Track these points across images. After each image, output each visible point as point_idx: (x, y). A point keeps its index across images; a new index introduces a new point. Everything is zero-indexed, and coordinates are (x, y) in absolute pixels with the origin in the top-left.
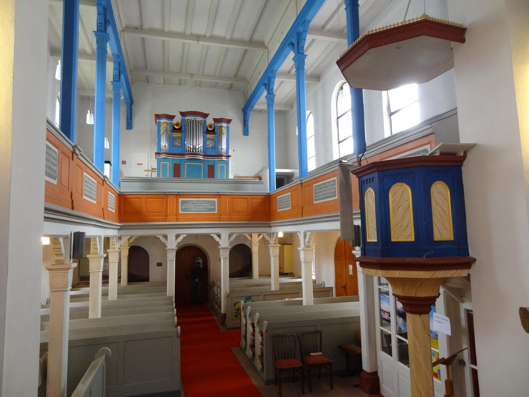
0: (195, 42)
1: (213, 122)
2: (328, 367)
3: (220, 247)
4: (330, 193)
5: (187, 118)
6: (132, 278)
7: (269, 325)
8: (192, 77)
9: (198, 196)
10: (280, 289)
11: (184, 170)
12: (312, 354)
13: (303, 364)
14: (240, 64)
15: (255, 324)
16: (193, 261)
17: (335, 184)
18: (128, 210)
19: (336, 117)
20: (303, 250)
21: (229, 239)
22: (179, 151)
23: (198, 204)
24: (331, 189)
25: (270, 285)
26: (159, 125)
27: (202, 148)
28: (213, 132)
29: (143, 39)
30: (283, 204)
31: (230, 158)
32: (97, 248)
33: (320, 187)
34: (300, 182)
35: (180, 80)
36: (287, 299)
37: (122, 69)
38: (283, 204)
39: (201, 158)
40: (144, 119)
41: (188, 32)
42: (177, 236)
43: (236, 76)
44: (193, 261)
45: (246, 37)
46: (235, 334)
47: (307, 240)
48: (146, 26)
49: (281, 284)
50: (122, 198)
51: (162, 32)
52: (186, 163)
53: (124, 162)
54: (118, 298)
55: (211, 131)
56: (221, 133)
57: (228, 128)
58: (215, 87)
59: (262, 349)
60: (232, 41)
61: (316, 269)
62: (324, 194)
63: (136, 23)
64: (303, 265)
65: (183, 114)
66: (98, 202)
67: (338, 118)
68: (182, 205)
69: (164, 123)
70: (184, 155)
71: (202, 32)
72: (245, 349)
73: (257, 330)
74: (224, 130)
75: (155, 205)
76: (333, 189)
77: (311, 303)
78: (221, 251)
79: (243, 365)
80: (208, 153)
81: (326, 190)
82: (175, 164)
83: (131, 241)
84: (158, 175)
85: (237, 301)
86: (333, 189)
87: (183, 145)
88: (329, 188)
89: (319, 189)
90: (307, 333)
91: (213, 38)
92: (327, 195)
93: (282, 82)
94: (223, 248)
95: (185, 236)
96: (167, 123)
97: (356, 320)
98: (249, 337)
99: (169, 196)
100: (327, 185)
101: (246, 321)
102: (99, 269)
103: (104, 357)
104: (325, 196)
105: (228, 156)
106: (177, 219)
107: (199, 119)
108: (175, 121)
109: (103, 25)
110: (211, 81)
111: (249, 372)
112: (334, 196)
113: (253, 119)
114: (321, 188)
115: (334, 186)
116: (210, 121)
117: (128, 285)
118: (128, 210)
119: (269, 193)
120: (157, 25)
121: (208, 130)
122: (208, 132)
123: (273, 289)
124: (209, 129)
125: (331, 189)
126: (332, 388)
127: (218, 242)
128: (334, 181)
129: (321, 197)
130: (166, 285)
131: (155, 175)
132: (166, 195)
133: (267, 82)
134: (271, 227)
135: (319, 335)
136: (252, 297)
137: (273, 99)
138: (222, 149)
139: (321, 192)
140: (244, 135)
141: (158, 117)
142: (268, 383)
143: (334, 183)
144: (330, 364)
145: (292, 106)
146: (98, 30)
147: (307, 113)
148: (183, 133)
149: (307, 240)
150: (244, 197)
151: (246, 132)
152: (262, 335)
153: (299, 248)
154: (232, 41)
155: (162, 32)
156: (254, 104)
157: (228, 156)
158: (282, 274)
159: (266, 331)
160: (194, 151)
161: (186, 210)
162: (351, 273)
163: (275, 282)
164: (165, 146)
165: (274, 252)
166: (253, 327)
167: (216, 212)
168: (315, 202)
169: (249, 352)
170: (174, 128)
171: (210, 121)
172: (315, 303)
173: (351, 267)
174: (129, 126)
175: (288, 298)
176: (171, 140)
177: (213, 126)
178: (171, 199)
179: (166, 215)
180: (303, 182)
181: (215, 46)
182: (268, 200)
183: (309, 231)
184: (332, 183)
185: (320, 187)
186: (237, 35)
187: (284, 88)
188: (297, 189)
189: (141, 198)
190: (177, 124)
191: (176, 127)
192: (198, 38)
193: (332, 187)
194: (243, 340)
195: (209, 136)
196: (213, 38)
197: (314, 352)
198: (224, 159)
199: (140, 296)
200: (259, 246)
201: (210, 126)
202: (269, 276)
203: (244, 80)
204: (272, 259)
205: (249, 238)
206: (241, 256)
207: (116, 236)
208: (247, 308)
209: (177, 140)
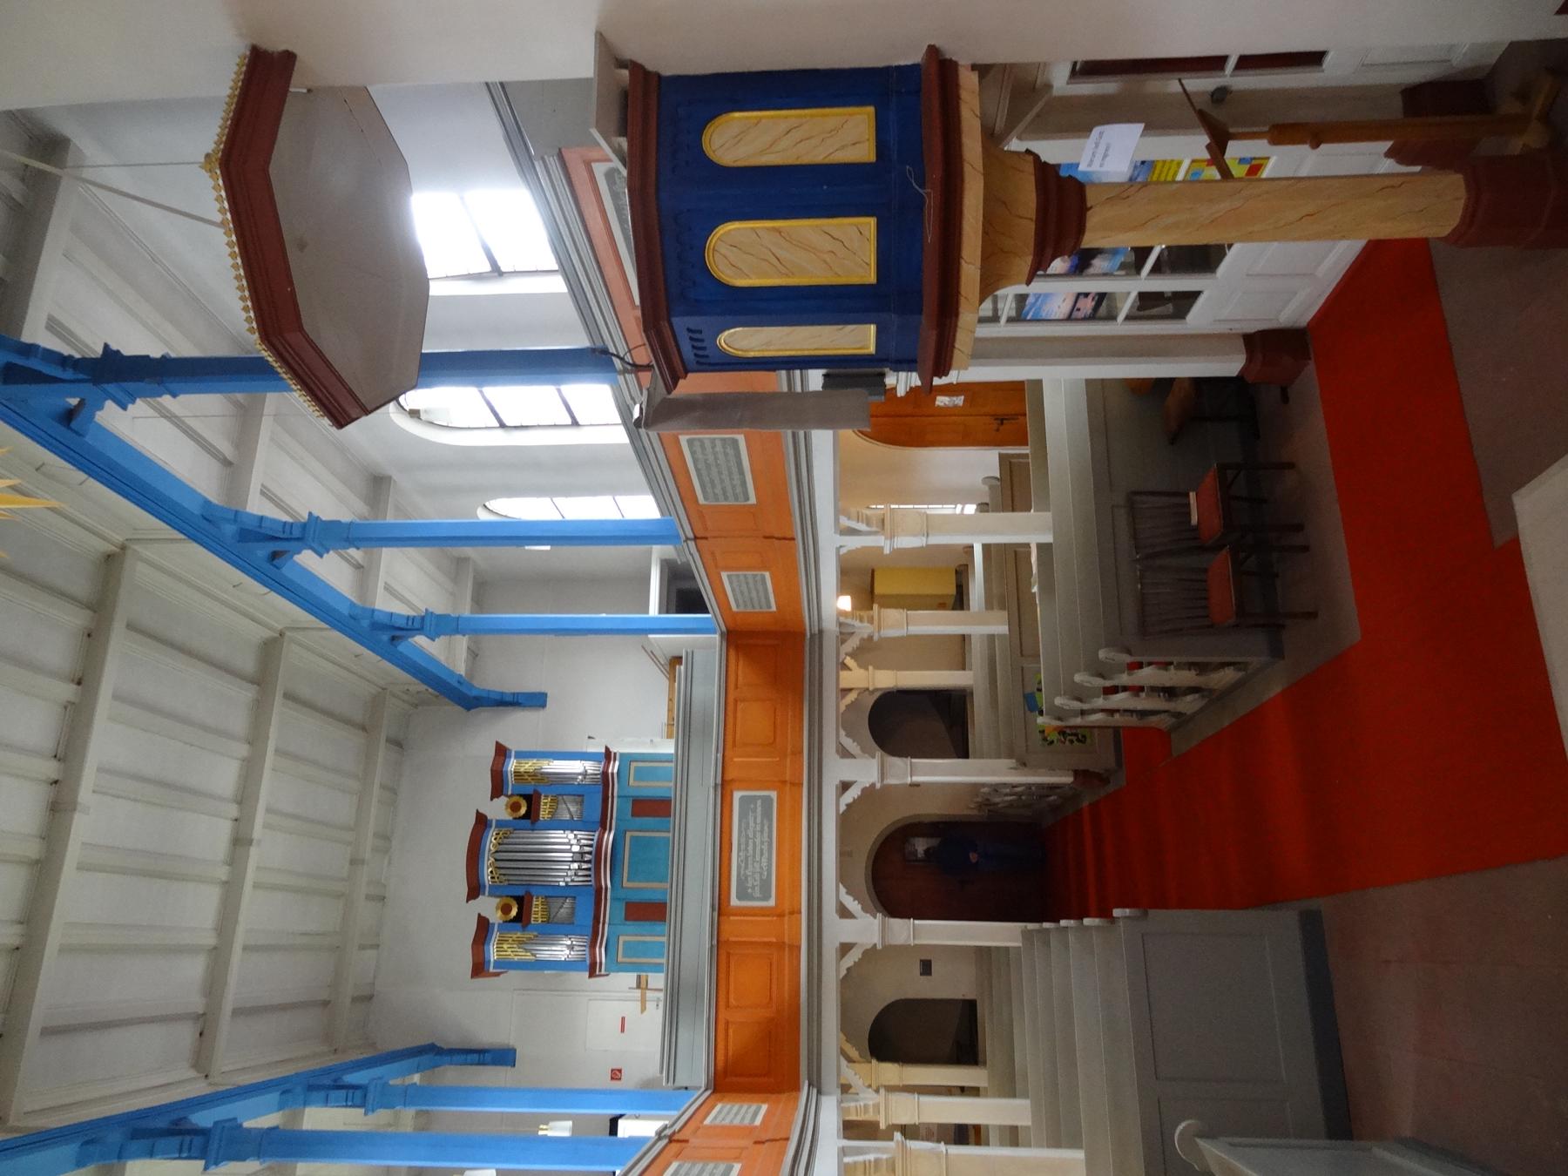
0: (253, 851)
1: (503, 800)
2: (1230, 474)
3: (878, 786)
4: (726, 454)
5: (487, 879)
6: (966, 1052)
7: (1110, 644)
8: (363, 862)
9: (725, 846)
10: (1002, 607)
11: (646, 889)
12: (1194, 520)
13: (1221, 547)
14: (327, 713)
15: (1108, 683)
16: (919, 866)
17: (701, 440)
18: (761, 1063)
19: (500, 432)
20: (892, 537)
21: (853, 757)
22: (586, 905)
23: (750, 848)
24: (715, 454)
25: (991, 638)
26: (505, 965)
27: (581, 834)
28: (532, 800)
29: (238, 1012)
30: (754, 594)
31: (613, 750)
32: (877, 1161)
33: (709, 485)
34: (692, 544)
35: (368, 897)
36: (1035, 589)
37: (327, 1081)
38: (754, 594)
39: (609, 838)
40: (484, 1012)
41: (222, 873)
42: (844, 913)
43: (364, 729)
44: (919, 866)
45: (247, 694)
46: (1134, 741)
47: (862, 527)
48: (197, 1003)
49: (989, 605)
50: (728, 1080)
51: (218, 956)
52: (625, 884)
53: (616, 1074)
54: (1025, 1095)
55: (529, 807)
56: (539, 777)
57: (521, 755)
58: (394, 791)
59: (1179, 667)
60: (256, 737)
61: (947, 502)
62: (730, 474)
63: (185, 1035)
64: (935, 540)
65: (474, 891)
66: (737, 1159)
67: (502, 426)
68: (753, 898)
69: (500, 949)
70: (598, 891)
71: (224, 829)
72: (1178, 715)
73: (1124, 679)
74: (529, 766)
75: (749, 979)
77: (1047, 516)
78: (891, 781)
79: (1226, 723)
80: (597, 816)
82: (627, 918)
83: (854, 1053)
84: (657, 968)
85: (1039, 737)
87: (570, 892)
88: (711, 458)
89: (713, 486)
90: (1135, 535)
91: (245, 797)
92: (733, 463)
93: (387, 588)
94: (883, 775)
95: (843, 890)
96: (501, 942)
97: (1096, 389)
98: (1143, 703)
99: (724, 937)
100: (701, 465)
101: (1098, 711)
102: (938, 1155)
103: (1202, 1143)
104: (735, 470)
105: (608, 755)
106: (792, 913)
107: (491, 840)
108: (495, 917)
109: (188, 1138)
110: (375, 800)
111: (1244, 705)
113: (499, 677)
114: (712, 482)
115: (708, 444)
116: (498, 810)
117: (985, 1063)
118: (761, 1063)
119: (722, 634)
120: (194, 969)
121: (527, 816)
122: (531, 815)
123: (1003, 629)
124: (523, 811)
125: (715, 454)
126: (1291, 466)
127: (864, 790)
128: (690, 442)
129: (737, 482)
130: (989, 948)
131: (657, 980)
132: (722, 949)
133: (387, 635)
134: (821, 632)
135: (1138, 498)
136: (1028, 690)
137: (439, 616)
138: (585, 774)
139: (722, 481)
140: (543, 705)
141: (479, 969)
142: (1277, 651)
143: (697, 444)
144: (1222, 468)
145: (461, 562)
146: (202, 1155)
147: (483, 516)
148: (533, 891)
149: (862, 527)
150: (730, 708)
151: (537, 701)
152: (1140, 666)
153: (887, 551)
154: (256, 737)
155: (218, 956)
156: (452, 673)
157: (608, 755)
158: (959, 601)
159: (1129, 652)
160: (588, 857)
161: (765, 885)
162: (959, 400)
163: (982, 623)
164: (571, 947)
165: (895, 623)
166: (1114, 690)
167: (774, 794)
168: (753, 500)
169: (1188, 704)
170: (518, 919)
171: (498, 810)
172: (1044, 507)
173: (942, 401)
174: (503, 1057)
175: (1030, 586)
176: (553, 929)
177: (515, 799)
178: (731, 932)
179: (780, 946)
180: (690, 535)
181: (269, 789)
182: (741, 639)
183: (837, 520)
184: (698, 450)
185: (709, 485)
186: (238, 721)
187: (406, 583)
188: (713, 553)
189: (727, 1023)
190: (506, 909)
191: (514, 912)
192: (240, 842)
193: (709, 450)
194: (1153, 720)
195: (544, 814)
196: (245, 797)
197: (1189, 514)
198: (614, 768)
199: (1022, 1029)
200: (877, 667)
201: (515, 807)
202: (964, 638)
203: (376, 703)
204: (915, 629)
205: (851, 697)
206: (906, 721)
207: (840, 1102)
208: (1060, 709)
209: (554, 911)
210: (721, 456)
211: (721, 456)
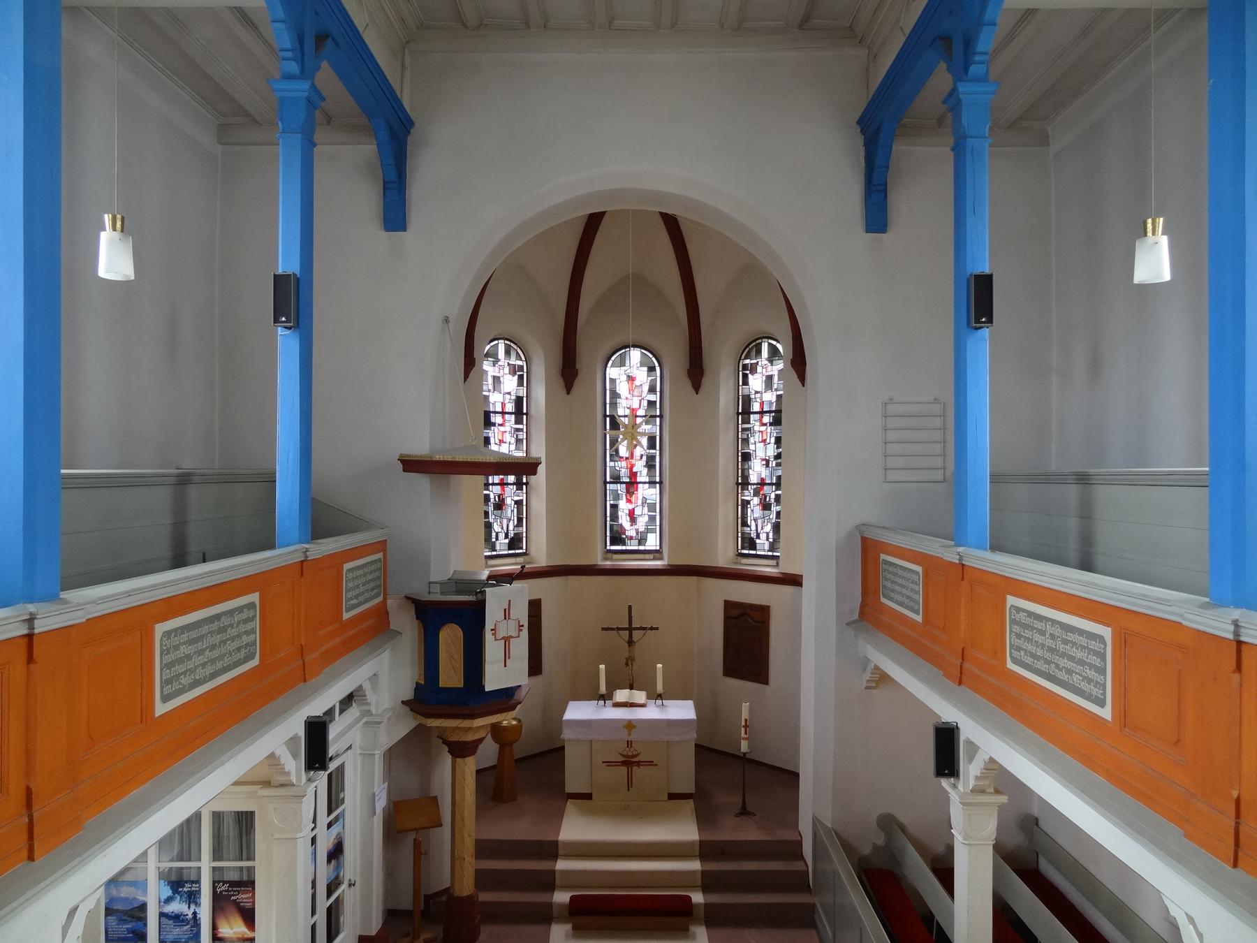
4: (239, 649)
24: (239, 636)
33: (194, 634)
62: (213, 661)
76: (247, 633)
81: (224, 642)
86: (247, 633)
88: (232, 632)
89: (190, 642)
100: (225, 621)
104: (219, 665)
112: (250, 657)
114: (200, 639)
115: (249, 626)
125: (239, 636)
128: (251, 606)
139: (200, 652)
184: (244, 615)
185: (194, 634)
193: (243, 628)
210: (236, 644)
211: (236, 644)
